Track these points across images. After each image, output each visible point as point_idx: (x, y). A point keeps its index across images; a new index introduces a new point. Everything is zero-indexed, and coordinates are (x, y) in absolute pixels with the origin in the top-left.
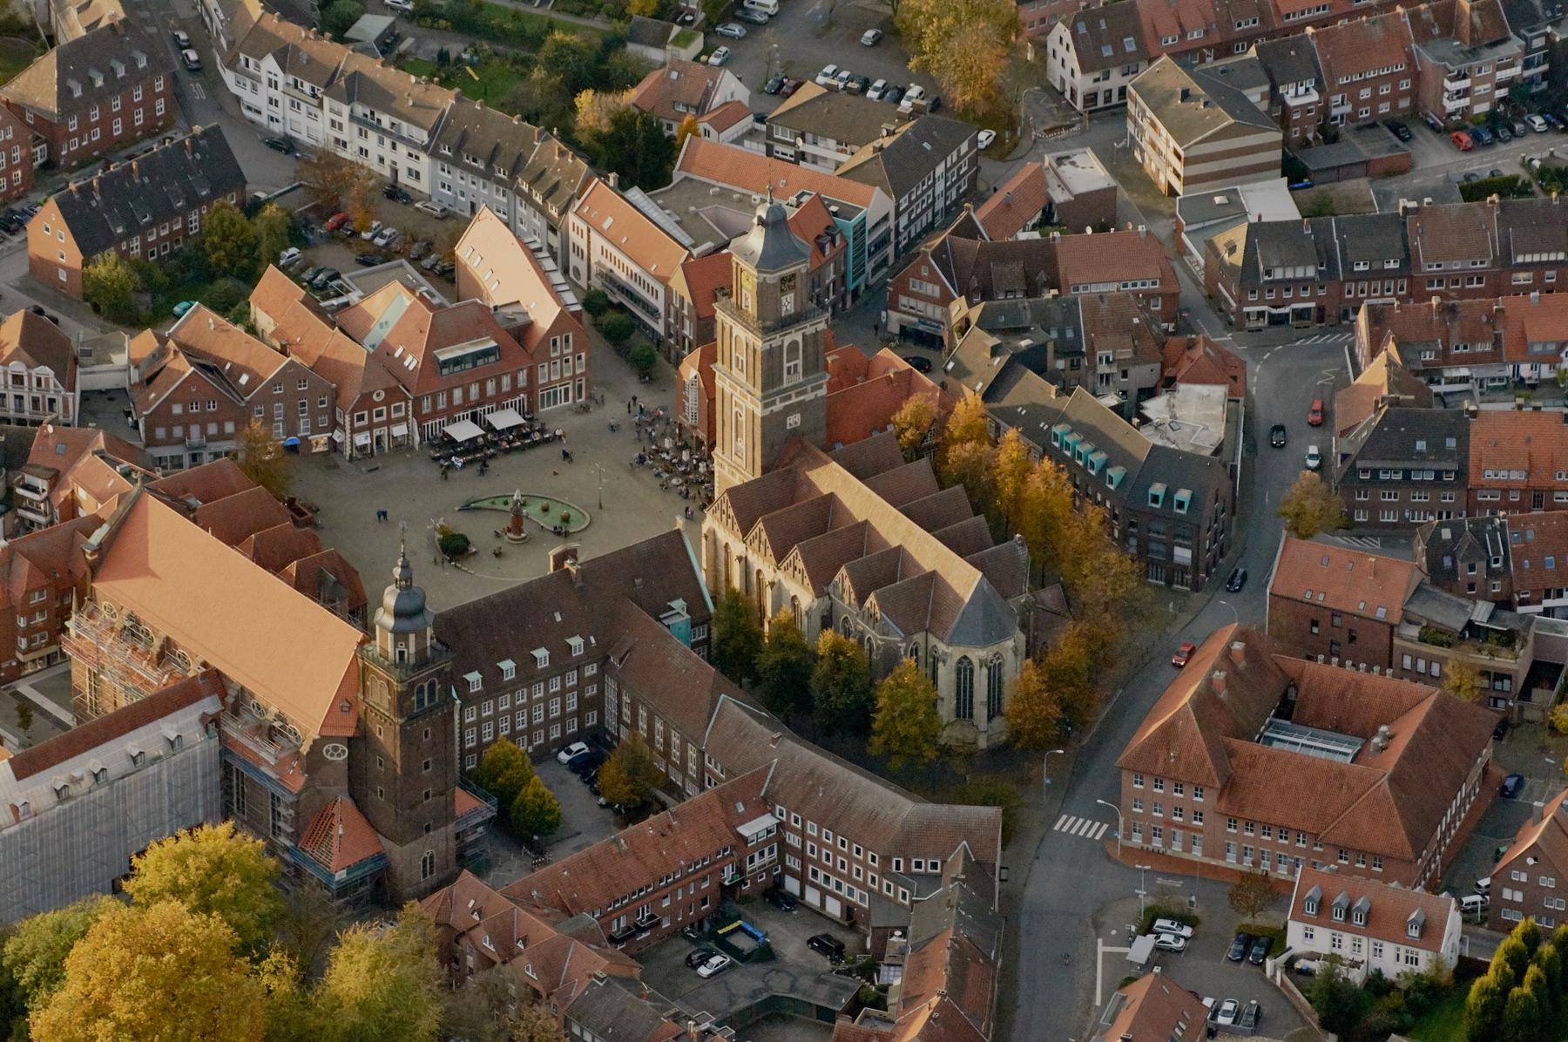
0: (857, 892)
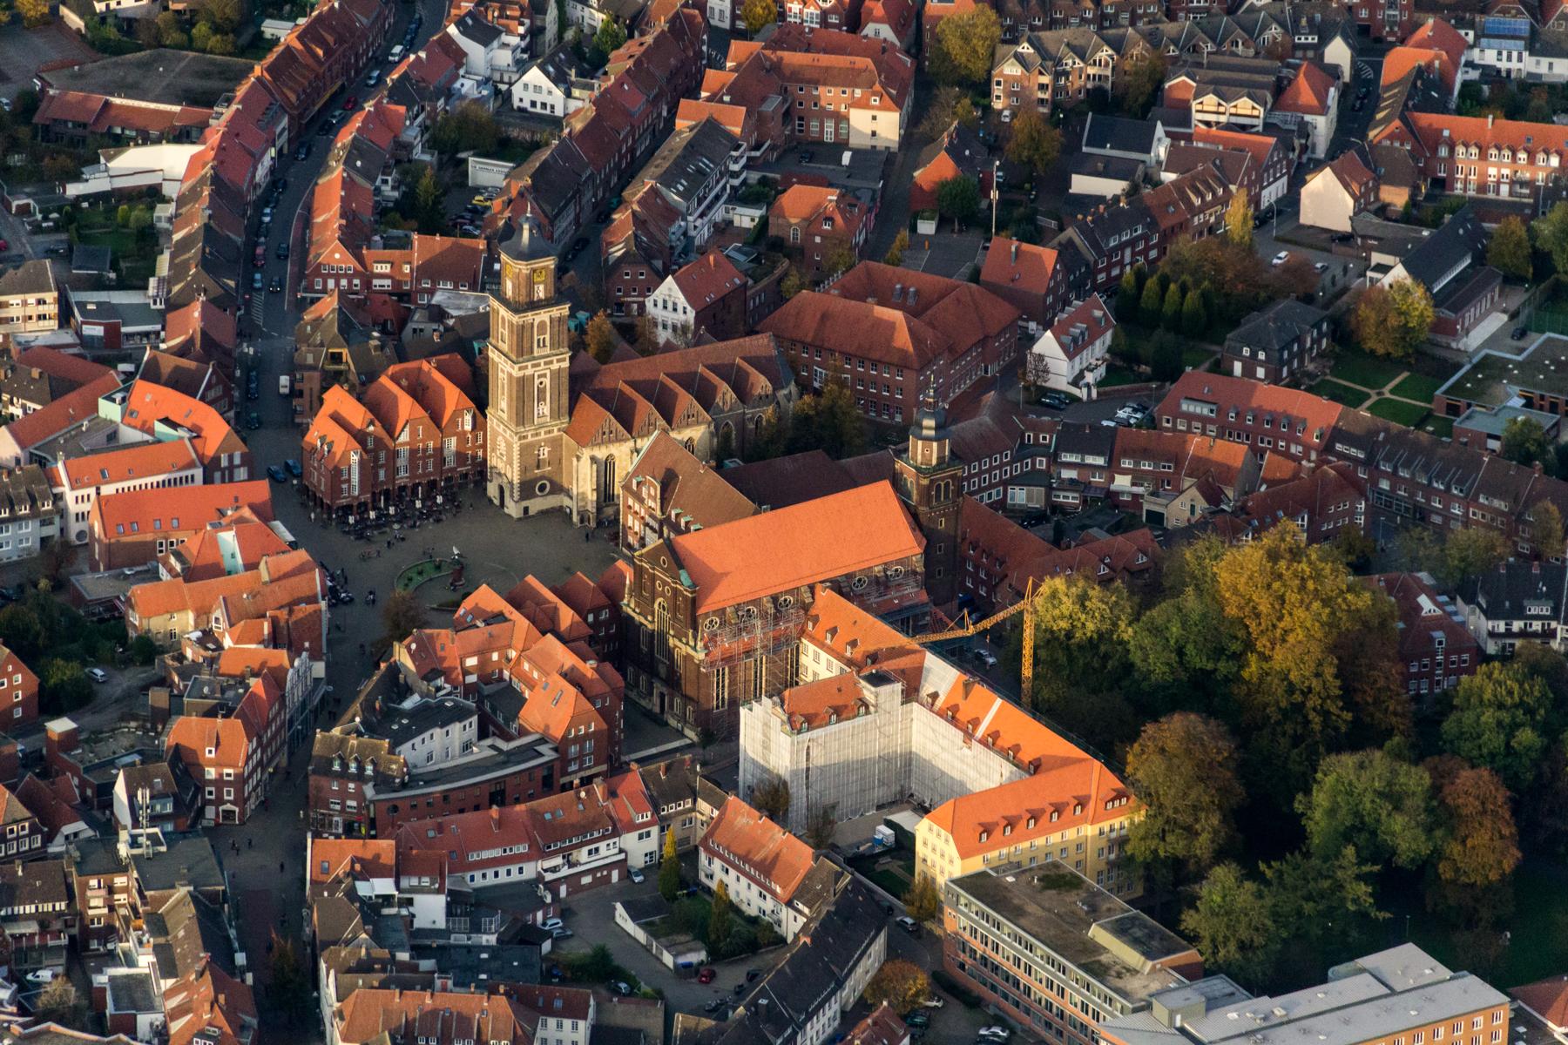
0: (994, 492)
